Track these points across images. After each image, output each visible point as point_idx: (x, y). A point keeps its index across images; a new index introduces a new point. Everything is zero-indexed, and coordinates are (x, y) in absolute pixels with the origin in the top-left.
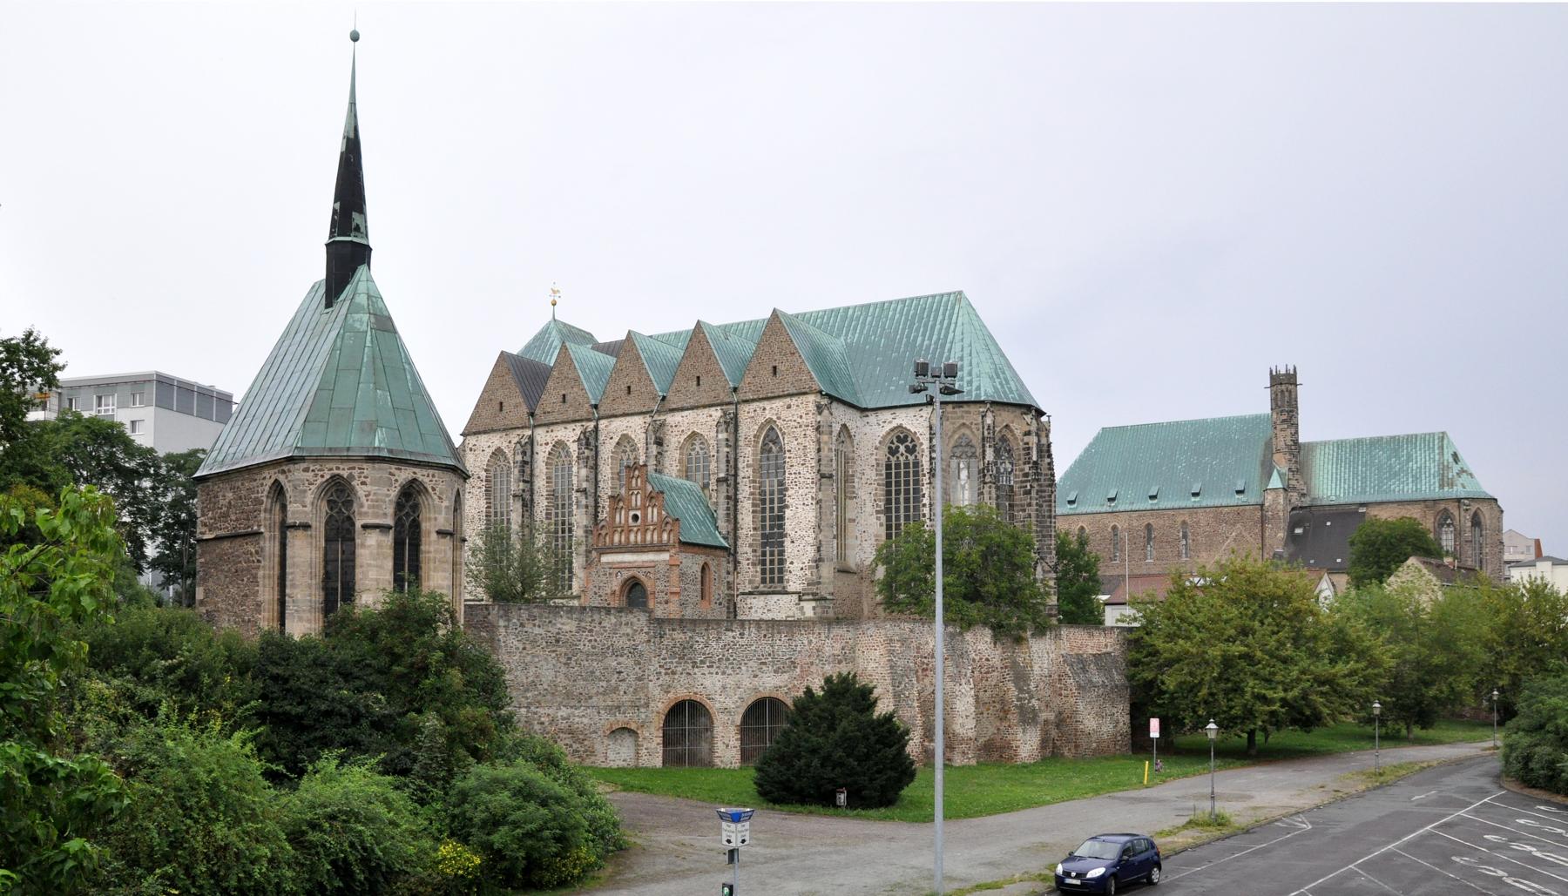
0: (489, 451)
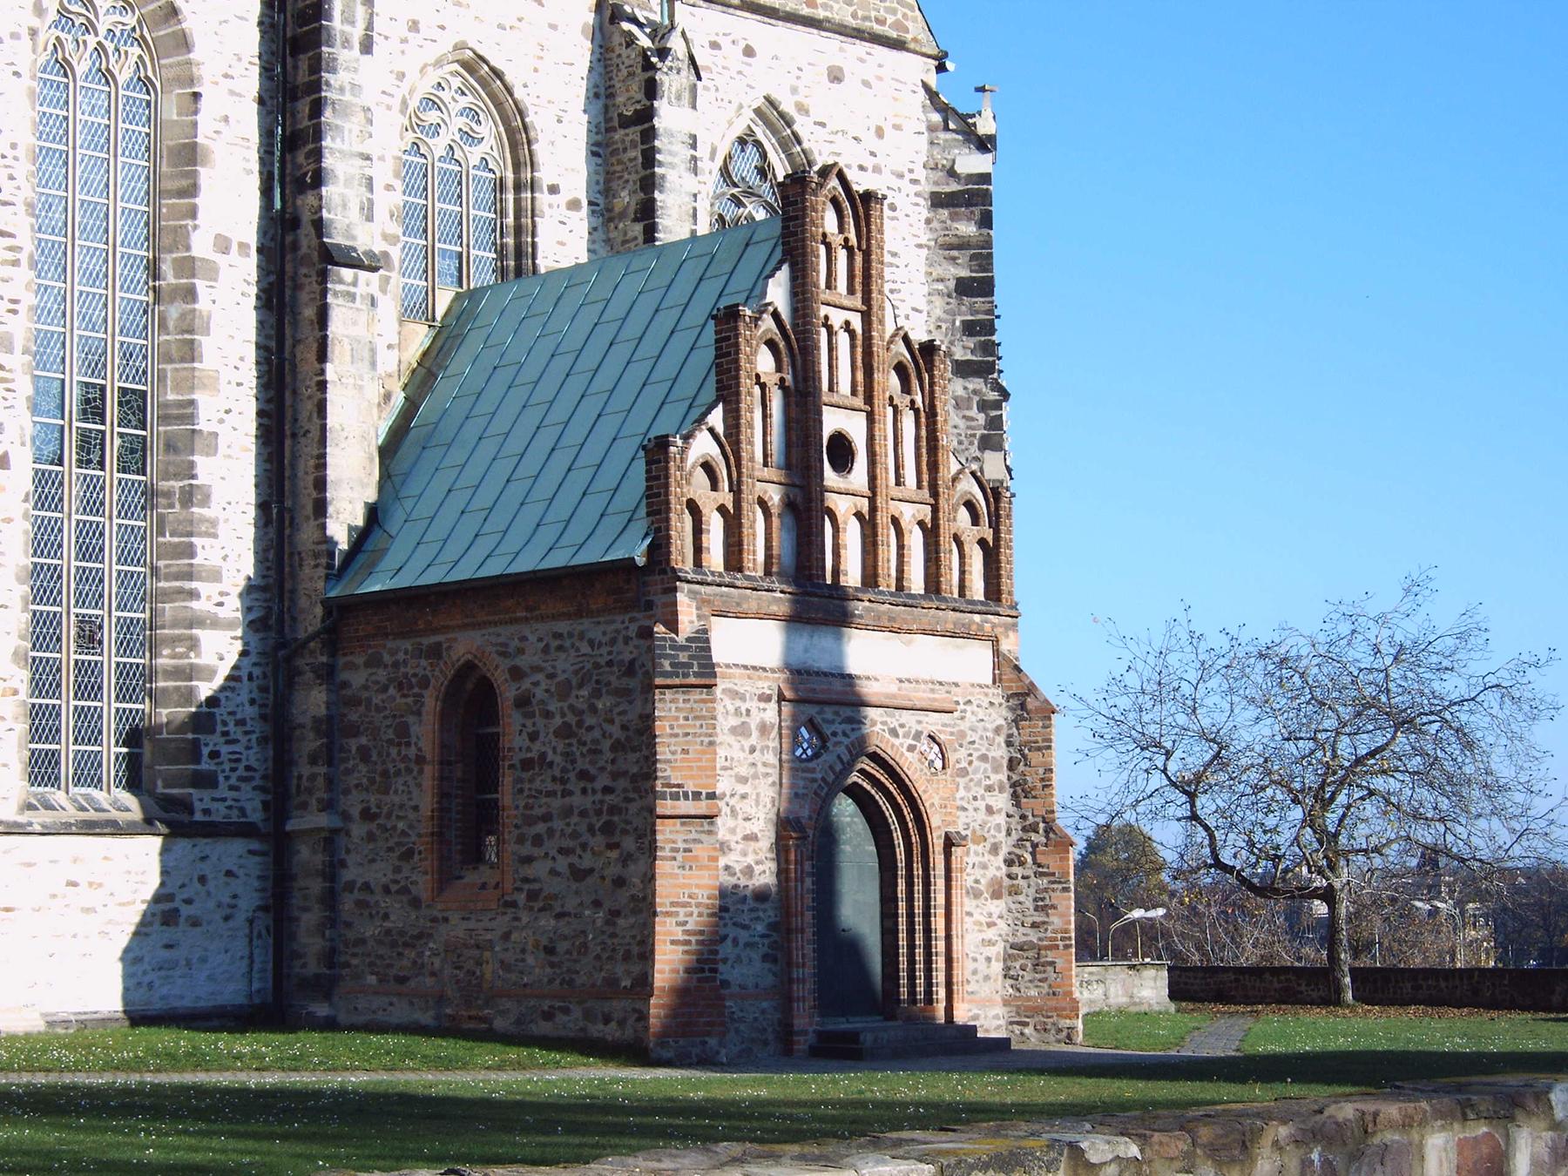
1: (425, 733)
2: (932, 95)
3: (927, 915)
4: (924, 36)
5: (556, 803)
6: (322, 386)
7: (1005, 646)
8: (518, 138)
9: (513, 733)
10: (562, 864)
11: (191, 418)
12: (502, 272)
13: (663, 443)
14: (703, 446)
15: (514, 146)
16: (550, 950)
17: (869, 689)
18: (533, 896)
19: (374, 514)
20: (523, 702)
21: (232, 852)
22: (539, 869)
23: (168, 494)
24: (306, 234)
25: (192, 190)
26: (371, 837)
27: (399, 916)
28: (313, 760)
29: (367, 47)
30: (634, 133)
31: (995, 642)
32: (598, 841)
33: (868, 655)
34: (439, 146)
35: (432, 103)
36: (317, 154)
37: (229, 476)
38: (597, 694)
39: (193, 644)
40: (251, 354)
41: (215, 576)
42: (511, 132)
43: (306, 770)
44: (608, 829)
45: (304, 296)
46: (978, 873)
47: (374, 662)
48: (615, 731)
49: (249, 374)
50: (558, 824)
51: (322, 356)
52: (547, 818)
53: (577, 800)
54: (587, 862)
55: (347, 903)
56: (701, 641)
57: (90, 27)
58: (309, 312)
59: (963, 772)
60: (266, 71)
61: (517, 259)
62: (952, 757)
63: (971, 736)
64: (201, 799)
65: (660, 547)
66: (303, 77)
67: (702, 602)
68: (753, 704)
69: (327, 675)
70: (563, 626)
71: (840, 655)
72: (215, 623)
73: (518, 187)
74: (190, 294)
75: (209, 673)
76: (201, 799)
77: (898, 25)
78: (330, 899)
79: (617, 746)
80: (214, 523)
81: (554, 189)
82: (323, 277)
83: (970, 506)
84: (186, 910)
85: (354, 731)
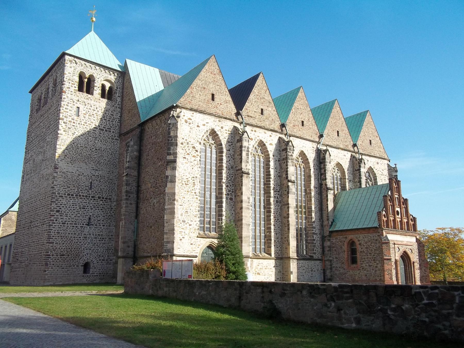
1: (345, 247)
5: (366, 257)
6: (327, 204)
9: (359, 248)
10: (367, 264)
13: (380, 212)
14: (384, 213)
16: (366, 275)
18: (363, 268)
20: (360, 244)
22: (364, 265)
23: (309, 218)
24: (324, 186)
26: (337, 261)
27: (342, 271)
29: (330, 163)
32: (373, 262)
38: (371, 243)
43: (327, 252)
44: (374, 260)
45: (323, 193)
48: (375, 248)
51: (327, 201)
52: (364, 259)
54: (371, 264)
55: (334, 269)
56: (386, 236)
58: (325, 195)
66: (322, 166)
67: (386, 232)
70: (366, 235)
79: (375, 250)
82: (327, 191)
83: (411, 220)
85: (334, 247)
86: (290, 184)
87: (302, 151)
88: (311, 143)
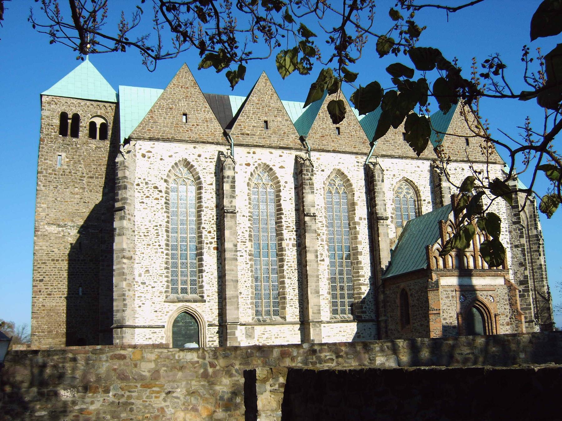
0: (173, 161)
1: (398, 301)
2: (503, 171)
3: (492, 329)
4: (501, 160)
7: (506, 277)
8: (417, 192)
11: (357, 249)
12: (416, 216)
15: (416, 194)
17: (477, 287)
18: (415, 329)
19: (390, 263)
20: (411, 295)
21: (370, 325)
23: (354, 263)
25: (354, 210)
28: (382, 307)
29: (383, 181)
30: (438, 188)
31: (504, 277)
33: (477, 282)
34: (402, 196)
35: (400, 188)
36: (375, 201)
37: (365, 259)
38: (422, 292)
39: (360, 288)
40: (367, 237)
41: (363, 276)
42: (415, 191)
46: (503, 321)
47: (390, 289)
49: (367, 241)
50: (418, 316)
51: (378, 237)
53: (421, 312)
54: (422, 323)
55: (389, 332)
56: (437, 282)
57: (335, 185)
58: (376, 229)
59: (498, 302)
60: (366, 188)
61: (418, 213)
62: (495, 299)
63: (500, 295)
64: (363, 316)
65: (429, 265)
66: (372, 188)
67: (437, 275)
68: (450, 292)
69: (383, 292)
70: (416, 281)
71: (471, 282)
72: (364, 285)
73: (418, 201)
74: (355, 228)
75: (364, 293)
76: (363, 316)
77: (495, 159)
78: (386, 332)
80: (362, 267)
81: (424, 200)
82: (377, 222)
84: (362, 335)
86: (307, 219)
87: (339, 170)
88: (353, 156)
